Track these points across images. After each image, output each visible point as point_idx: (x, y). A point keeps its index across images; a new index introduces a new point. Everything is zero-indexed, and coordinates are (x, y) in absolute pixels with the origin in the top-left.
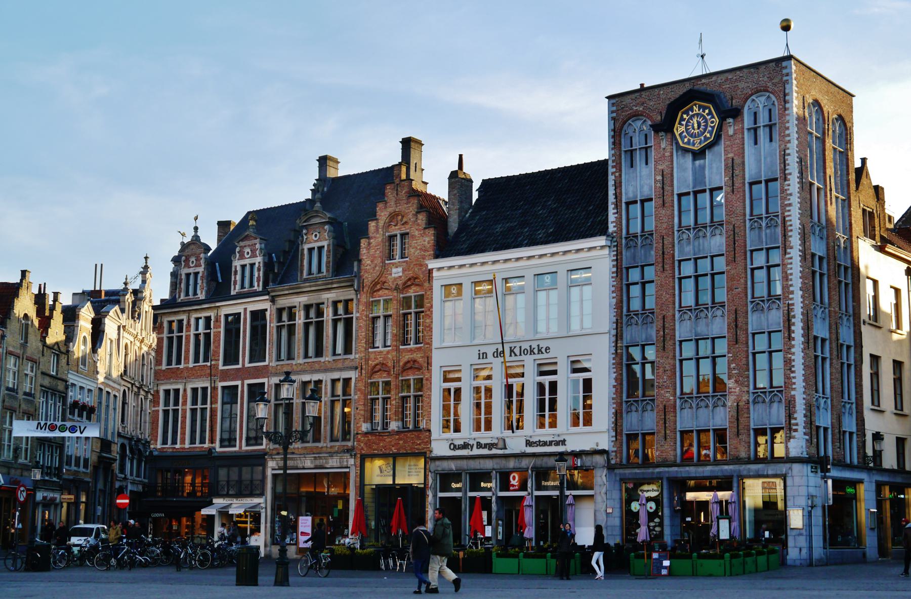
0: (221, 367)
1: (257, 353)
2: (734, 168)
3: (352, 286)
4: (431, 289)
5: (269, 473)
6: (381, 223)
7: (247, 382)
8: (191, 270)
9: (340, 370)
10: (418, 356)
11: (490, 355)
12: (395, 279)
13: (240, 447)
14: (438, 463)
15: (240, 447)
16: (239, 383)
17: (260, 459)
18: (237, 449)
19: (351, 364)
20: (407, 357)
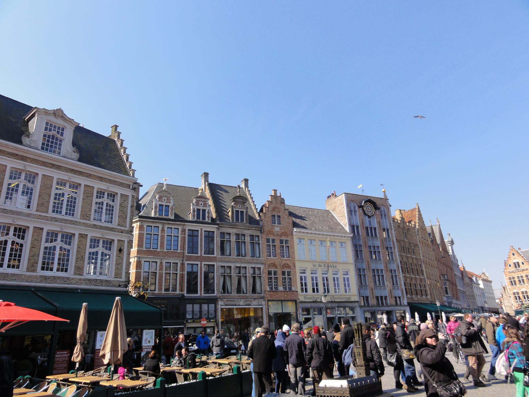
0: (186, 254)
1: (210, 251)
2: (379, 223)
3: (261, 230)
4: (293, 238)
5: (219, 307)
6: (270, 209)
7: (203, 263)
8: (164, 204)
9: (254, 263)
10: (288, 262)
11: (317, 266)
12: (277, 232)
13: (201, 294)
14: (303, 304)
15: (201, 294)
16: (199, 263)
17: (214, 301)
18: (199, 295)
19: (260, 262)
20: (284, 262)
